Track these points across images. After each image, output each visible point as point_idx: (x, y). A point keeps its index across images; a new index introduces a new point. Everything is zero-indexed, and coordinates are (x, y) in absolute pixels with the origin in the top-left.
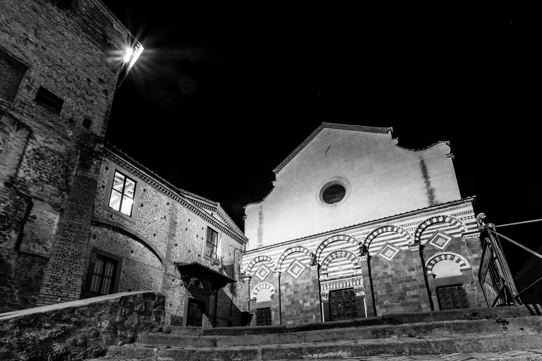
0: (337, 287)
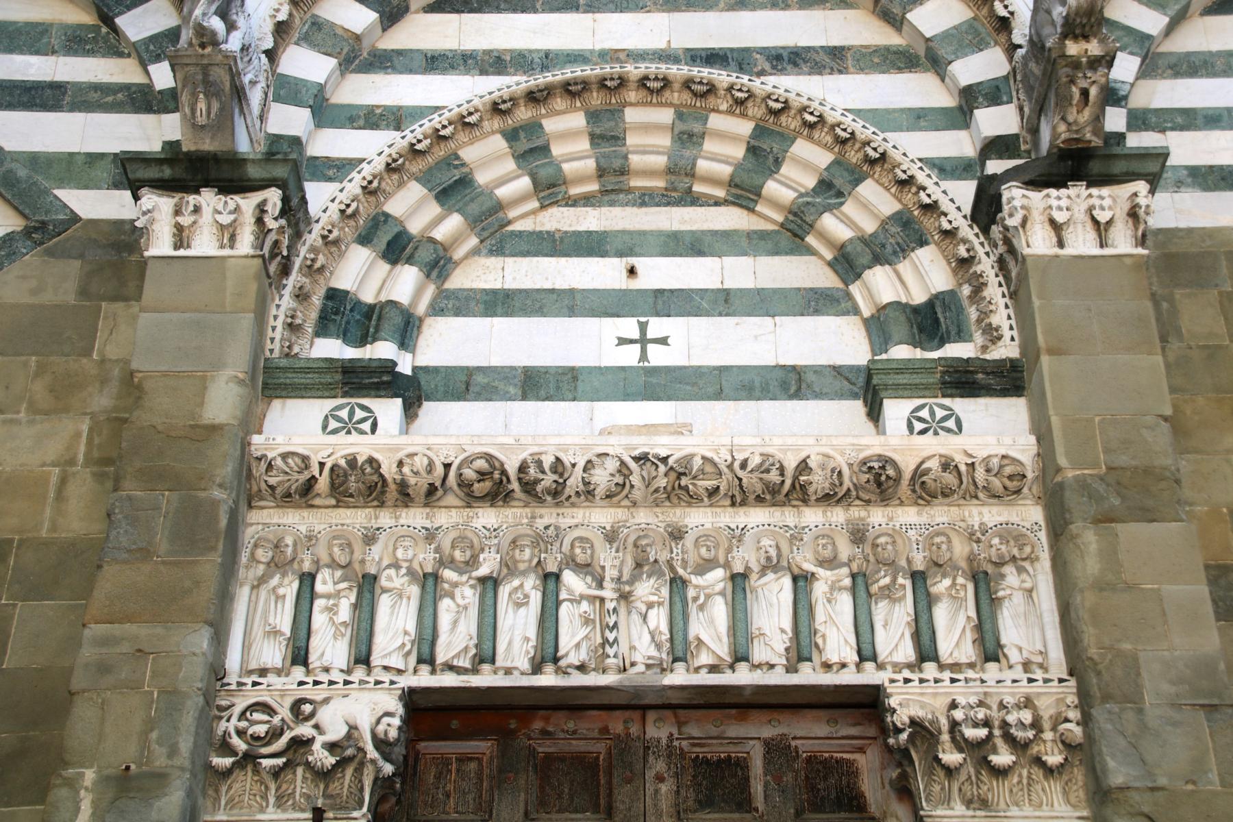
0: (573, 636)
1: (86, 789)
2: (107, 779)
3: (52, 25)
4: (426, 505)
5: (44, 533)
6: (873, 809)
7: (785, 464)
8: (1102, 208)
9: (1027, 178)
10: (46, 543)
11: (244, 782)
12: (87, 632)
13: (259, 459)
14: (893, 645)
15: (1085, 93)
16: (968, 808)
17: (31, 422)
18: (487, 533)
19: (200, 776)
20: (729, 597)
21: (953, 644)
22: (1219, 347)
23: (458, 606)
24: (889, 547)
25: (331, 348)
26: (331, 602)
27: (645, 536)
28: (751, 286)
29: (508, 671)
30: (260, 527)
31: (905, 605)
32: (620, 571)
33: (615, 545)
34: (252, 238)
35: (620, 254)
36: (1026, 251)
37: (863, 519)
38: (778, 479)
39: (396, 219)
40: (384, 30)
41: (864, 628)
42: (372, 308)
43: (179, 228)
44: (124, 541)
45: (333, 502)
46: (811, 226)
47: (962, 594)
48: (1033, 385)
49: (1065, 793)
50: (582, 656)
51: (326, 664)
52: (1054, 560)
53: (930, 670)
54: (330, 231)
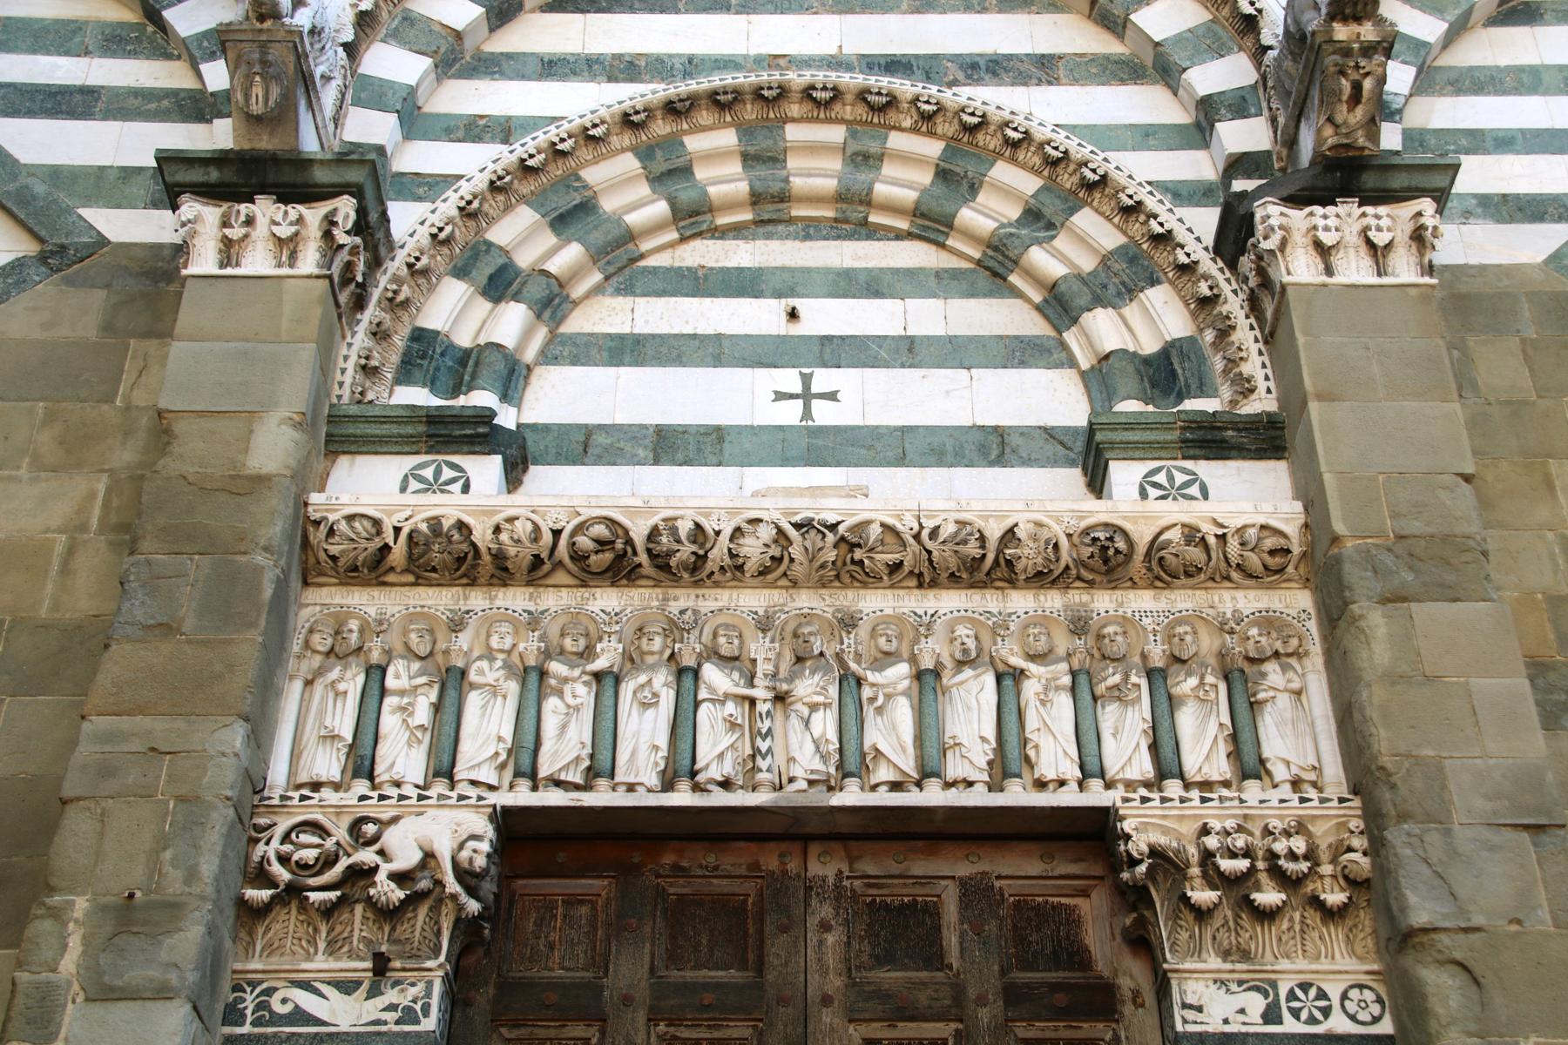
0: (715, 746)
1: (76, 921)
2: (104, 908)
3: (87, 23)
4: (529, 583)
5: (43, 613)
6: (1101, 967)
7: (987, 533)
8: (1379, 229)
9: (1285, 194)
10: (45, 626)
11: (287, 922)
12: (86, 726)
13: (317, 523)
14: (1125, 758)
15: (1357, 87)
16: (1225, 961)
17: (34, 481)
18: (606, 618)
19: (230, 912)
20: (916, 700)
21: (1202, 757)
22: (1524, 403)
23: (568, 706)
24: (1119, 638)
25: (417, 396)
26: (406, 700)
27: (808, 624)
28: (941, 332)
29: (631, 788)
30: (318, 608)
31: (1141, 710)
32: (777, 667)
33: (769, 634)
34: (318, 255)
35: (779, 295)
36: (1286, 279)
37: (1085, 605)
38: (977, 553)
39: (501, 248)
40: (492, 30)
41: (1089, 738)
42: (467, 353)
43: (227, 243)
44: (139, 614)
45: (411, 578)
46: (1016, 263)
47: (1213, 695)
48: (1297, 442)
49: (1349, 941)
50: (728, 768)
51: (396, 777)
52: (1328, 654)
53: (1173, 788)
54: (418, 259)
